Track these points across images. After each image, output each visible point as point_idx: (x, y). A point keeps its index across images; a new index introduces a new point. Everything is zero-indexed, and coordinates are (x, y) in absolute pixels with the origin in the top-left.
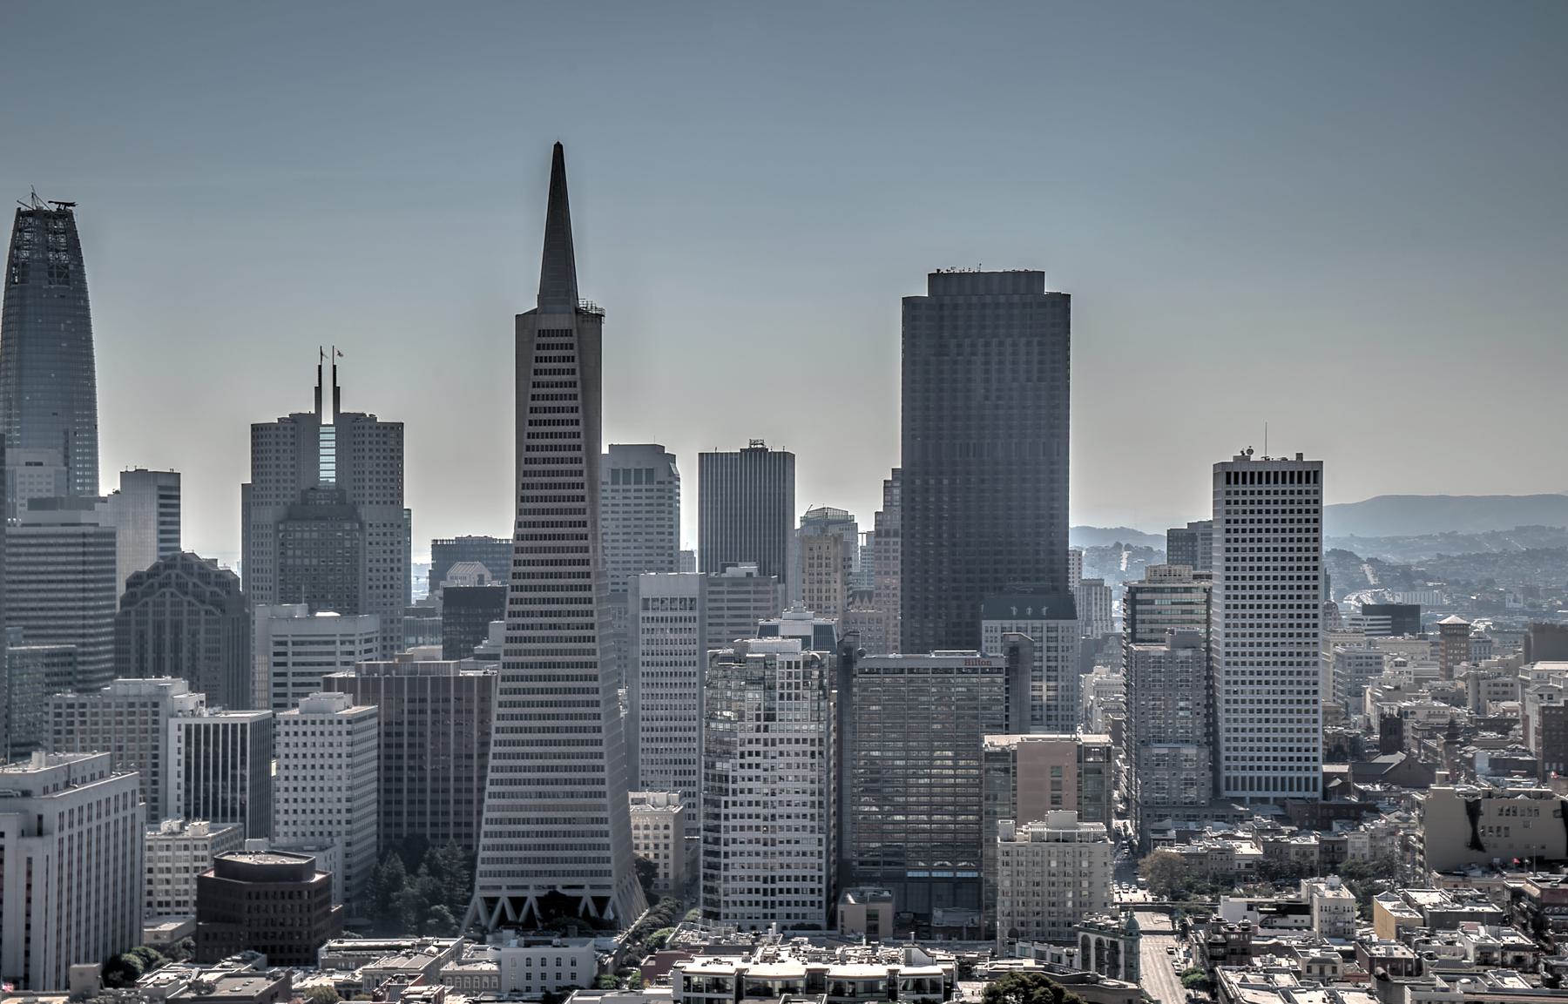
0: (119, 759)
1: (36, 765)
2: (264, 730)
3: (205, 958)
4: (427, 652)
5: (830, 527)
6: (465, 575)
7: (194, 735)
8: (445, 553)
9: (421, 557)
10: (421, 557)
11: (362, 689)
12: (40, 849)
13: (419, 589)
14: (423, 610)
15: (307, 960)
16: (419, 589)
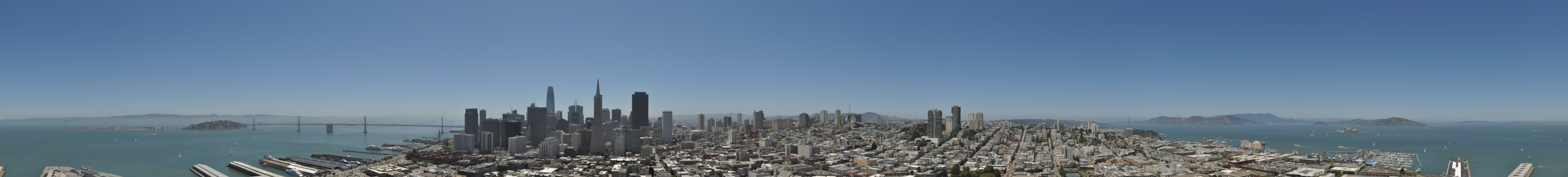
0: (557, 138)
1: (550, 138)
2: (570, 135)
3: (565, 157)
4: (586, 129)
5: (625, 117)
6: (589, 121)
7: (564, 136)
8: (587, 119)
9: (585, 119)
10: (585, 119)
11: (579, 132)
12: (551, 146)
13: (585, 122)
14: (585, 124)
15: (575, 157)
16: (585, 122)
